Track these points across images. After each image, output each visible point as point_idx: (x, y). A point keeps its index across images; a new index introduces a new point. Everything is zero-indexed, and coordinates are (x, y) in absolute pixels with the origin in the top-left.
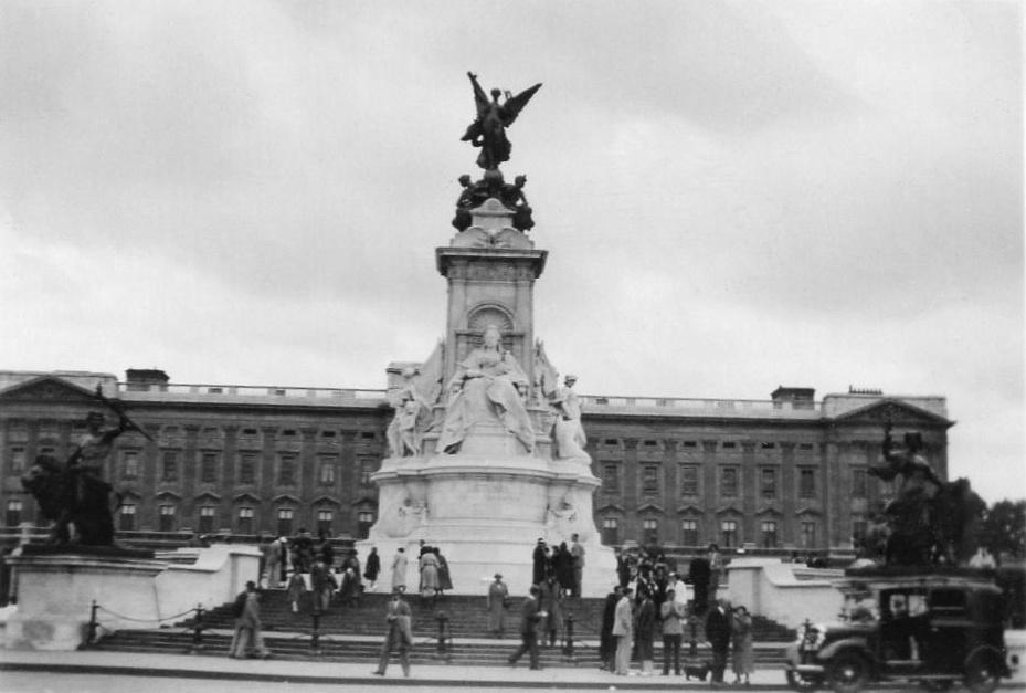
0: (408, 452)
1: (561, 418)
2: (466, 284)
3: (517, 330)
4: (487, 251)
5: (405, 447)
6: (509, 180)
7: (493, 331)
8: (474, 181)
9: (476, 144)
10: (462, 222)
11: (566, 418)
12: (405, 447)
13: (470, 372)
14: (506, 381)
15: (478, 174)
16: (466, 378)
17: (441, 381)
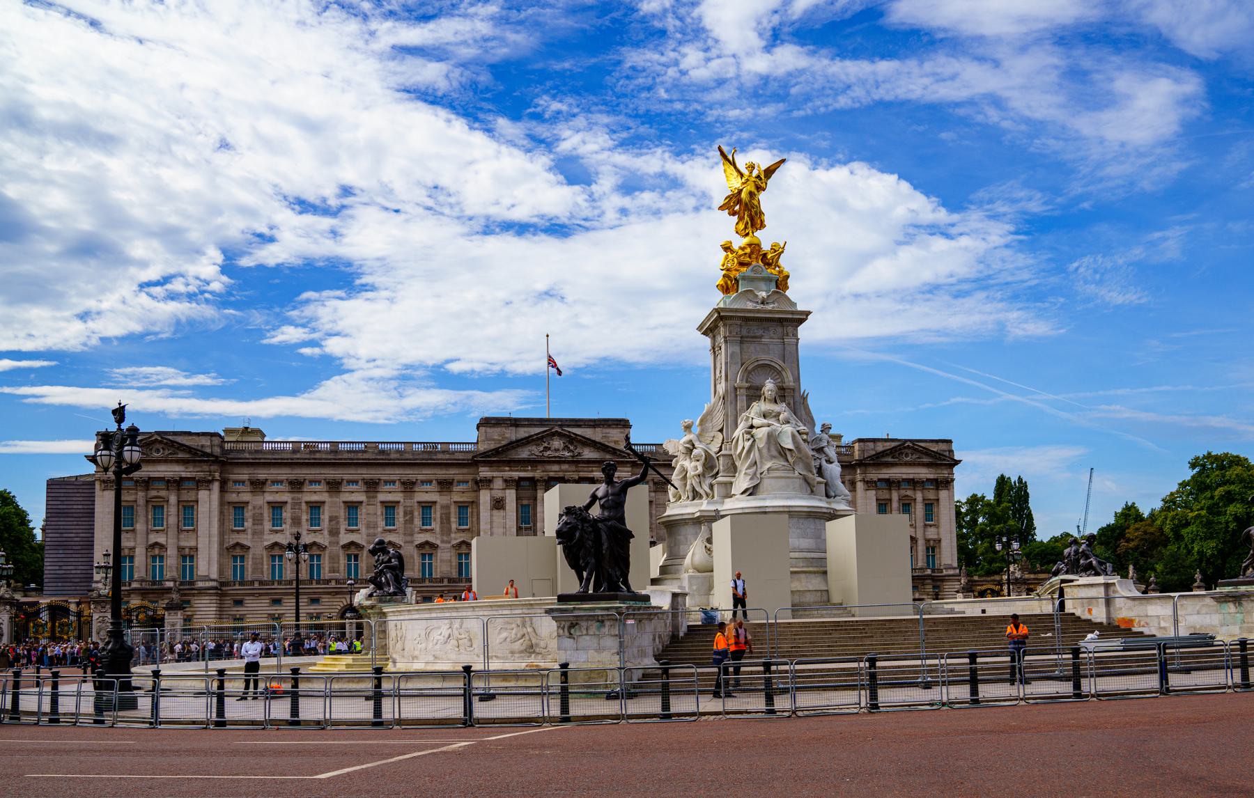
0: (696, 495)
1: (824, 463)
2: (741, 342)
3: (789, 381)
4: (758, 311)
5: (694, 490)
6: (766, 247)
7: (769, 386)
8: (735, 247)
9: (733, 214)
10: (727, 287)
11: (829, 461)
12: (694, 490)
13: (757, 422)
14: (788, 429)
15: (739, 242)
16: (752, 427)
17: (721, 431)
